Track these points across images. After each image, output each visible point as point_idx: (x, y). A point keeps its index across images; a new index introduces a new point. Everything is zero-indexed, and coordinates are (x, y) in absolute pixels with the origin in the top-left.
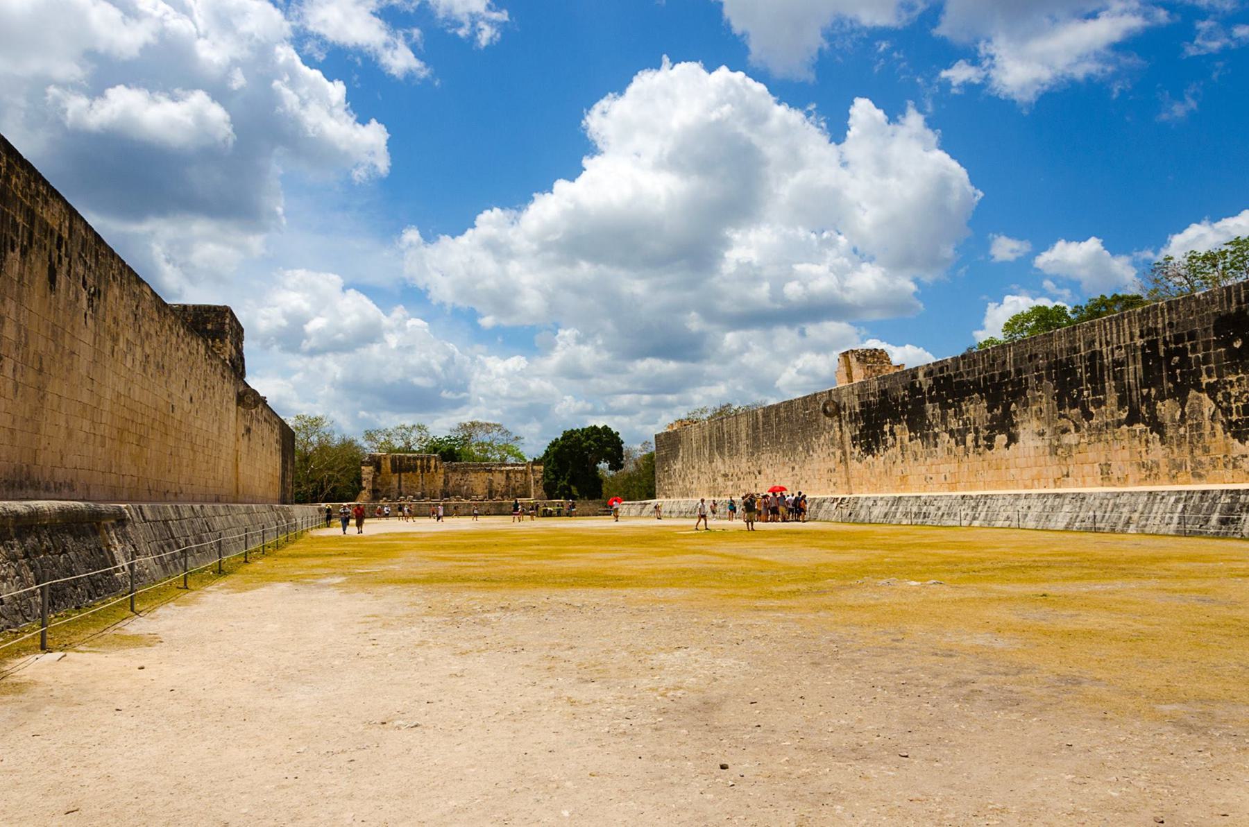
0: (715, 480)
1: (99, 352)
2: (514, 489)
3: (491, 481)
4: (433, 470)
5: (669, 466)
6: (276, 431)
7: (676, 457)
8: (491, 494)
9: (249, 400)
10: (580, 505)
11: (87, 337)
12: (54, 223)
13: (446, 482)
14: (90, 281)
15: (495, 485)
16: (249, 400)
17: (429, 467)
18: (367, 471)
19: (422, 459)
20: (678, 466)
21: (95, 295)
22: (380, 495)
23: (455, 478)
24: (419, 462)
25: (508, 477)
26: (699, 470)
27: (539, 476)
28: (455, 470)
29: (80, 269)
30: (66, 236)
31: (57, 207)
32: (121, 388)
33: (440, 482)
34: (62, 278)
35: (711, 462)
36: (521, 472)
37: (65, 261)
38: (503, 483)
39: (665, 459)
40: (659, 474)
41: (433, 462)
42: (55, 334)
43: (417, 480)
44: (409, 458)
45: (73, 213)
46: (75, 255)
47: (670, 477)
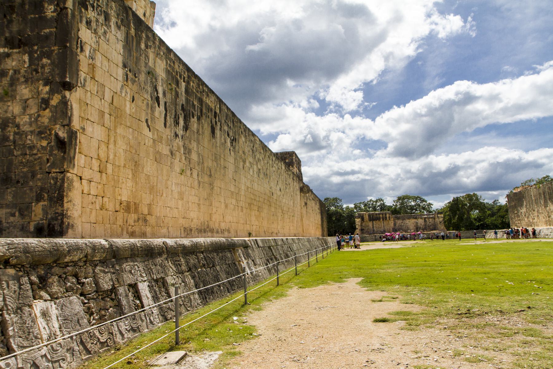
0: (549, 217)
1: (237, 167)
2: (429, 226)
3: (417, 223)
4: (388, 219)
5: (518, 211)
6: (318, 204)
7: (521, 205)
8: (417, 229)
9: (305, 189)
10: (463, 233)
11: (231, 160)
12: (212, 106)
13: (395, 224)
14: (231, 134)
15: (419, 224)
16: (305, 189)
17: (386, 218)
18: (358, 221)
19: (383, 214)
20: (523, 210)
21: (233, 140)
22: (365, 231)
23: (399, 222)
24: (381, 216)
25: (425, 221)
26: (538, 211)
27: (441, 219)
28: (398, 218)
29: (226, 128)
30: (218, 111)
31: (213, 98)
32: (248, 184)
33: (392, 225)
34: (218, 132)
35: (546, 206)
36: (432, 218)
37: (219, 124)
38: (423, 224)
39: (515, 207)
40: (511, 215)
41: (388, 215)
42: (216, 158)
43: (378, 225)
44: (376, 214)
45: (220, 101)
46: (223, 121)
47: (518, 216)
